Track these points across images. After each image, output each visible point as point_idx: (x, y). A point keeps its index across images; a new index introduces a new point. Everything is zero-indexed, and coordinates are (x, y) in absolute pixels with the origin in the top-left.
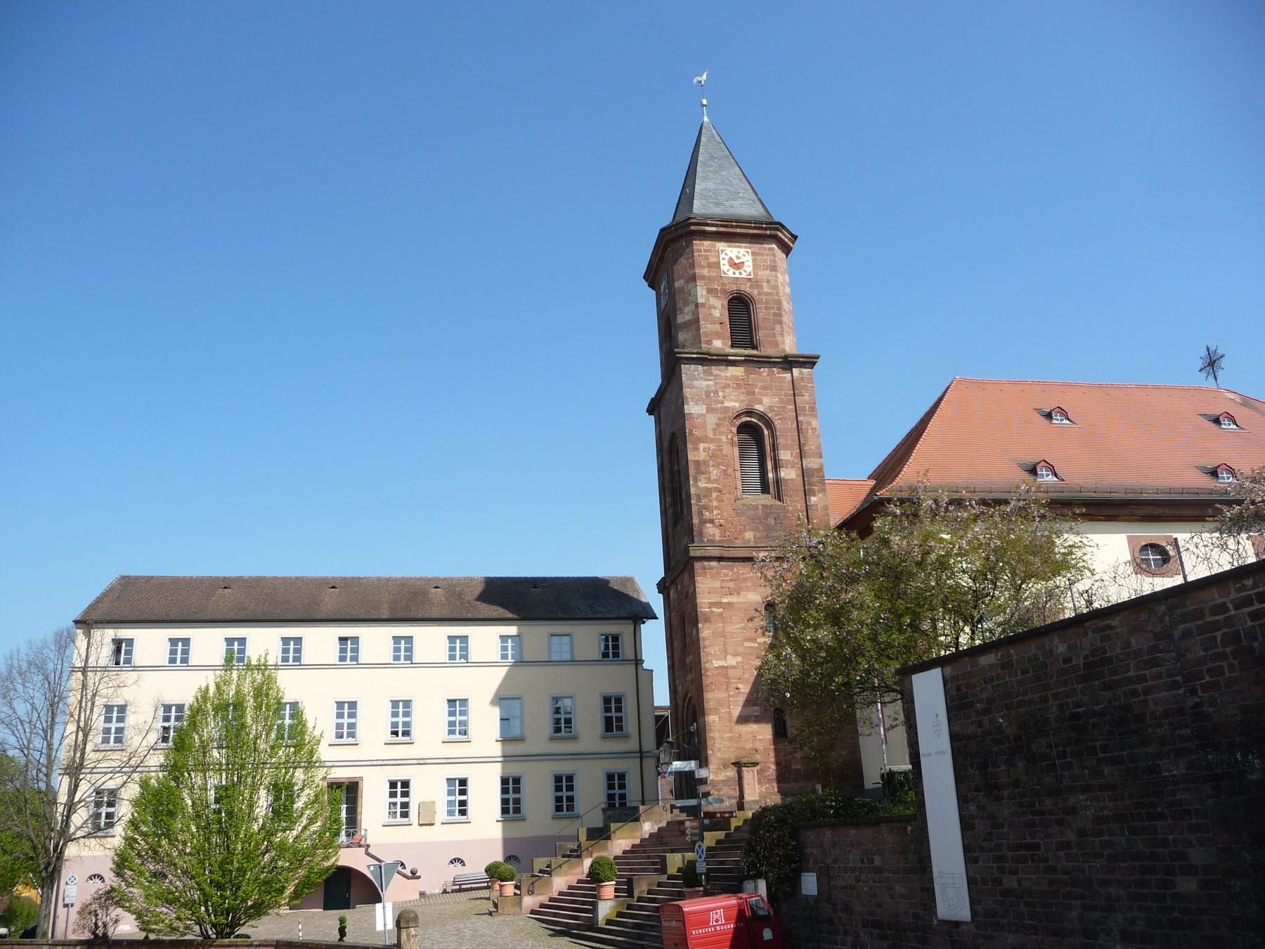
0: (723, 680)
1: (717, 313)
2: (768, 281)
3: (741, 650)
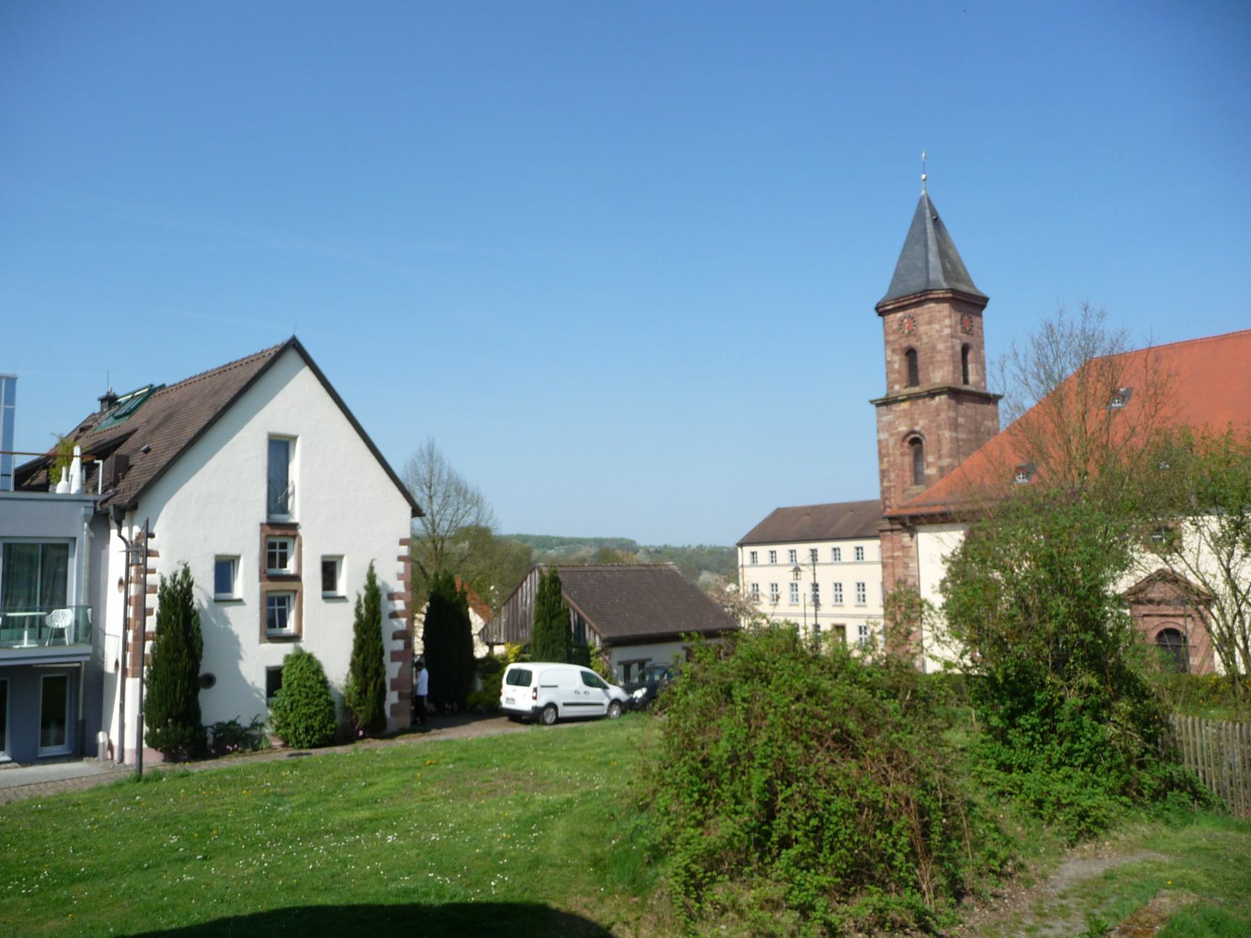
1: (896, 366)
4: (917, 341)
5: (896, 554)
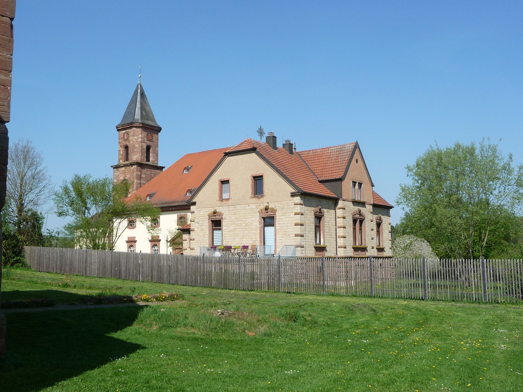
1: (121, 152)
4: (129, 143)
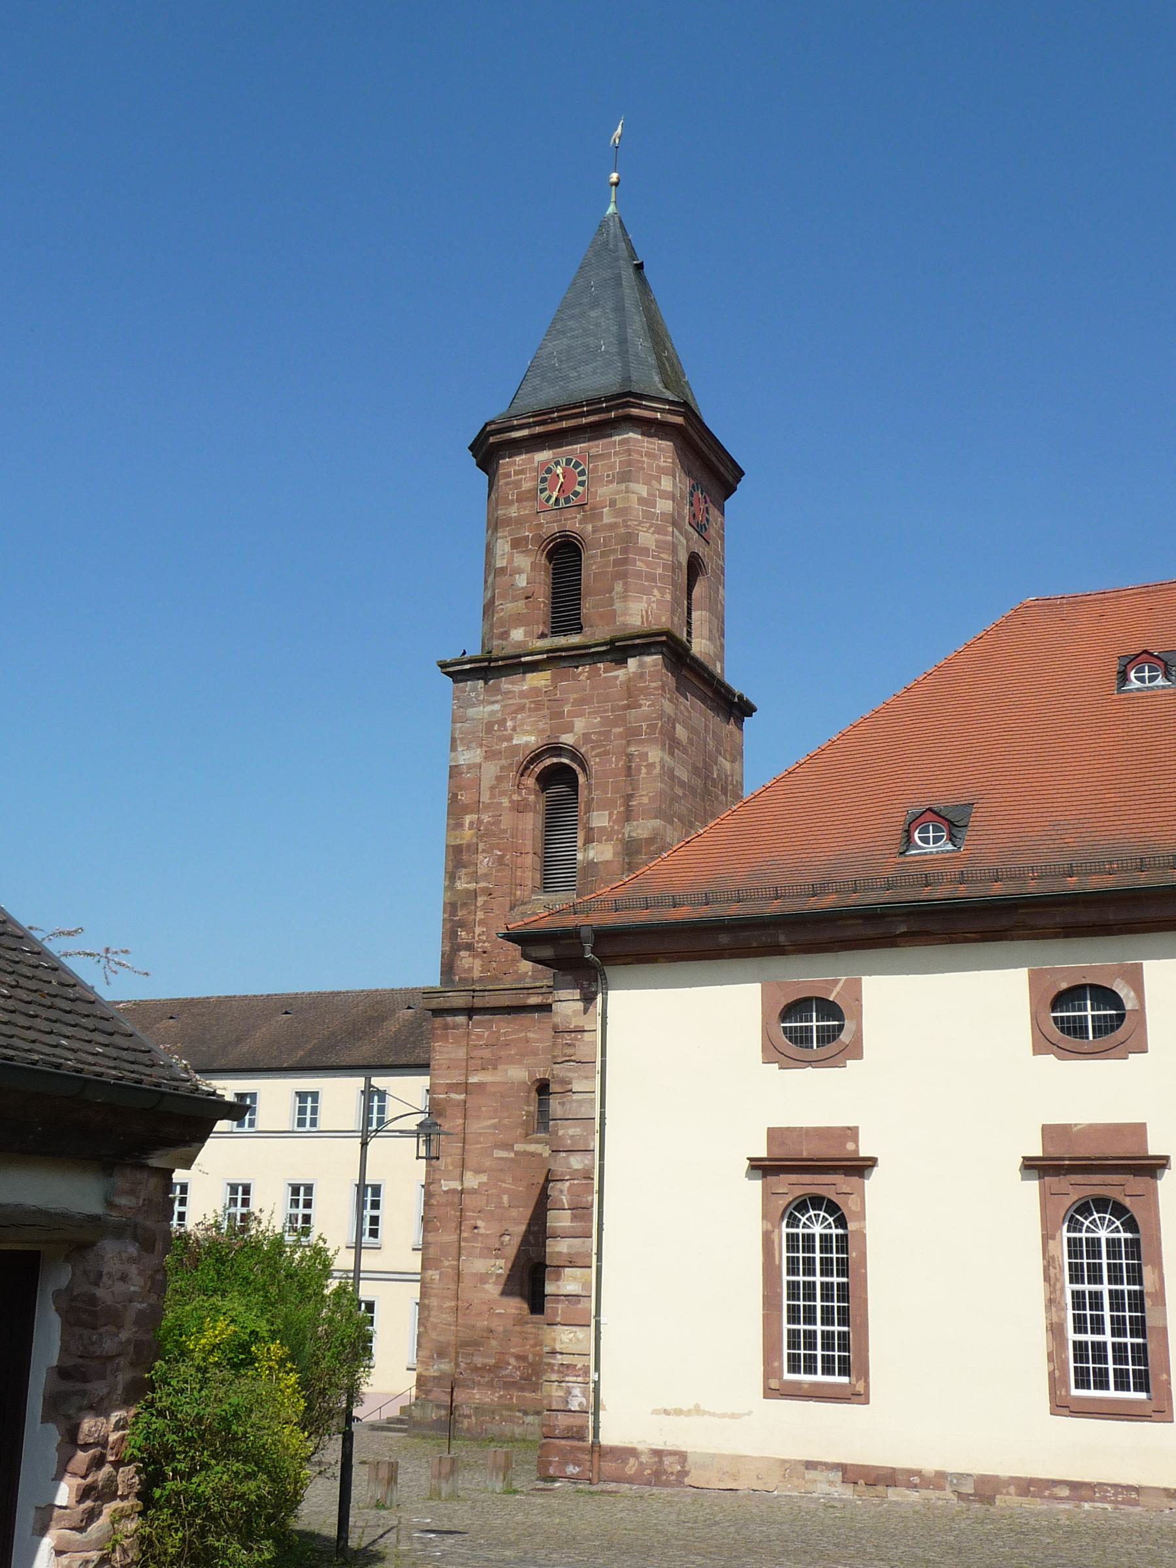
0: (453, 1213)
1: (522, 581)
2: (613, 503)
3: (488, 1163)
4: (583, 521)
5: (473, 1079)
